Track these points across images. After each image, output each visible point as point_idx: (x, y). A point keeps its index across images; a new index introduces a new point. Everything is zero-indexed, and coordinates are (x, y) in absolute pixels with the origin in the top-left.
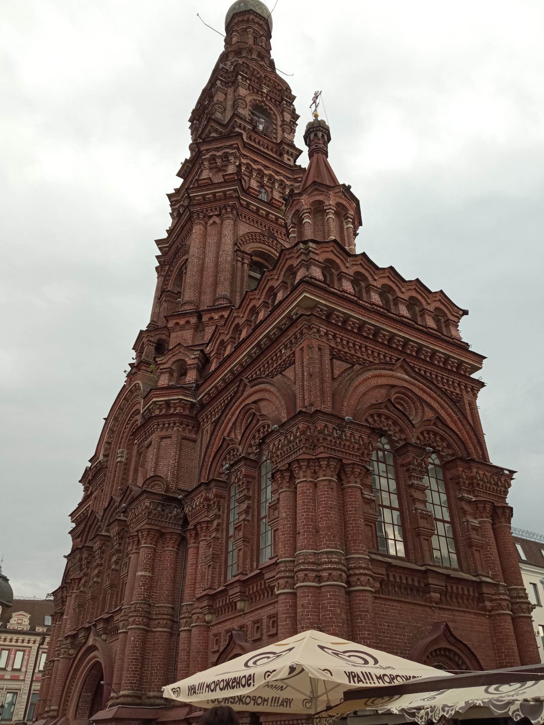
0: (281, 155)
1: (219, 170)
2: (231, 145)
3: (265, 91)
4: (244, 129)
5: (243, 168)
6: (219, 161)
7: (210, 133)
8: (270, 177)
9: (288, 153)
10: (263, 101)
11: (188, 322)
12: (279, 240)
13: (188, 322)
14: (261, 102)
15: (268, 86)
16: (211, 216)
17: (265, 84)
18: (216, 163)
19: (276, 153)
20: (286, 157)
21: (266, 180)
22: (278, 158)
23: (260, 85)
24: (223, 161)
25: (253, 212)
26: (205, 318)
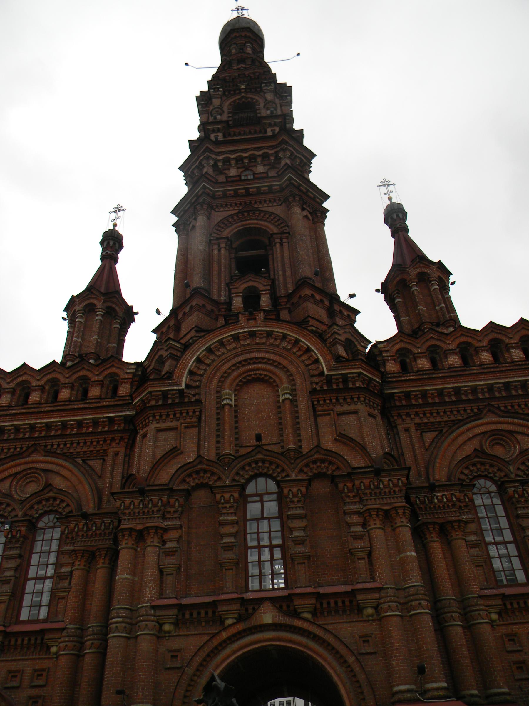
0: (266, 132)
3: (243, 87)
4: (219, 131)
5: (220, 164)
9: (270, 125)
10: (243, 97)
12: (262, 209)
15: (244, 82)
17: (240, 82)
19: (260, 132)
21: (246, 161)
23: (237, 86)
25: (232, 196)
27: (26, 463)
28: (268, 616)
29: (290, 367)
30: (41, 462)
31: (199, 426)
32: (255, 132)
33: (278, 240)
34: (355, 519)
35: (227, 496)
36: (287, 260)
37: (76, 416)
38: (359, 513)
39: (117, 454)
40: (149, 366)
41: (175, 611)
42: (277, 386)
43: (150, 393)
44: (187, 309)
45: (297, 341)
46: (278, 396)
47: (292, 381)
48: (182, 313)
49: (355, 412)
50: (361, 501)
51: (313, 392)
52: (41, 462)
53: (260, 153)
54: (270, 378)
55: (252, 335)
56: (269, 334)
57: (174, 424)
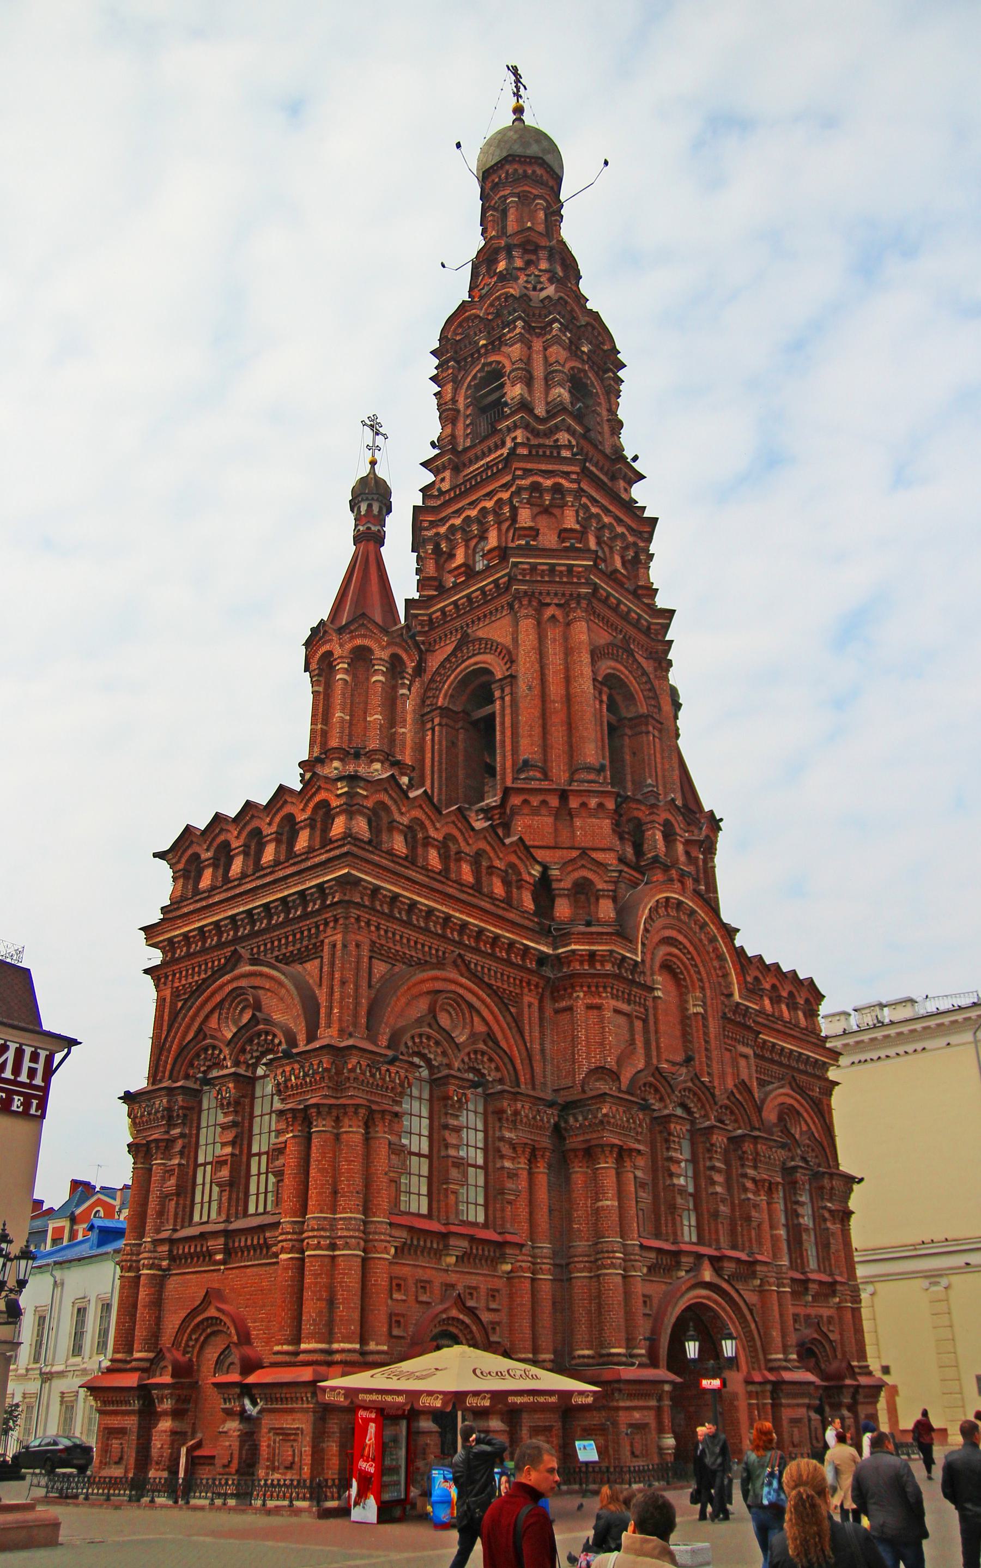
0: (613, 478)
1: (546, 511)
2: (568, 473)
6: (547, 498)
7: (516, 427)
8: (611, 528)
10: (585, 371)
11: (544, 802)
13: (544, 802)
14: (580, 370)
16: (548, 605)
18: (541, 497)
19: (606, 474)
20: (622, 484)
22: (609, 484)
24: (553, 499)
26: (574, 803)
27: (445, 980)
28: (708, 1275)
29: (702, 969)
30: (461, 985)
31: (645, 1021)
32: (601, 469)
33: (651, 729)
34: (749, 1184)
35: (678, 1127)
36: (660, 774)
37: (495, 926)
38: (754, 1180)
39: (530, 1005)
40: (560, 880)
41: (653, 1255)
42: (686, 987)
43: (611, 951)
44: (593, 802)
45: (713, 940)
46: (687, 1002)
47: (703, 989)
48: (580, 800)
49: (746, 1057)
50: (755, 1167)
51: (724, 1017)
52: (461, 985)
53: (620, 530)
54: (682, 973)
55: (680, 903)
56: (692, 912)
57: (625, 1007)
